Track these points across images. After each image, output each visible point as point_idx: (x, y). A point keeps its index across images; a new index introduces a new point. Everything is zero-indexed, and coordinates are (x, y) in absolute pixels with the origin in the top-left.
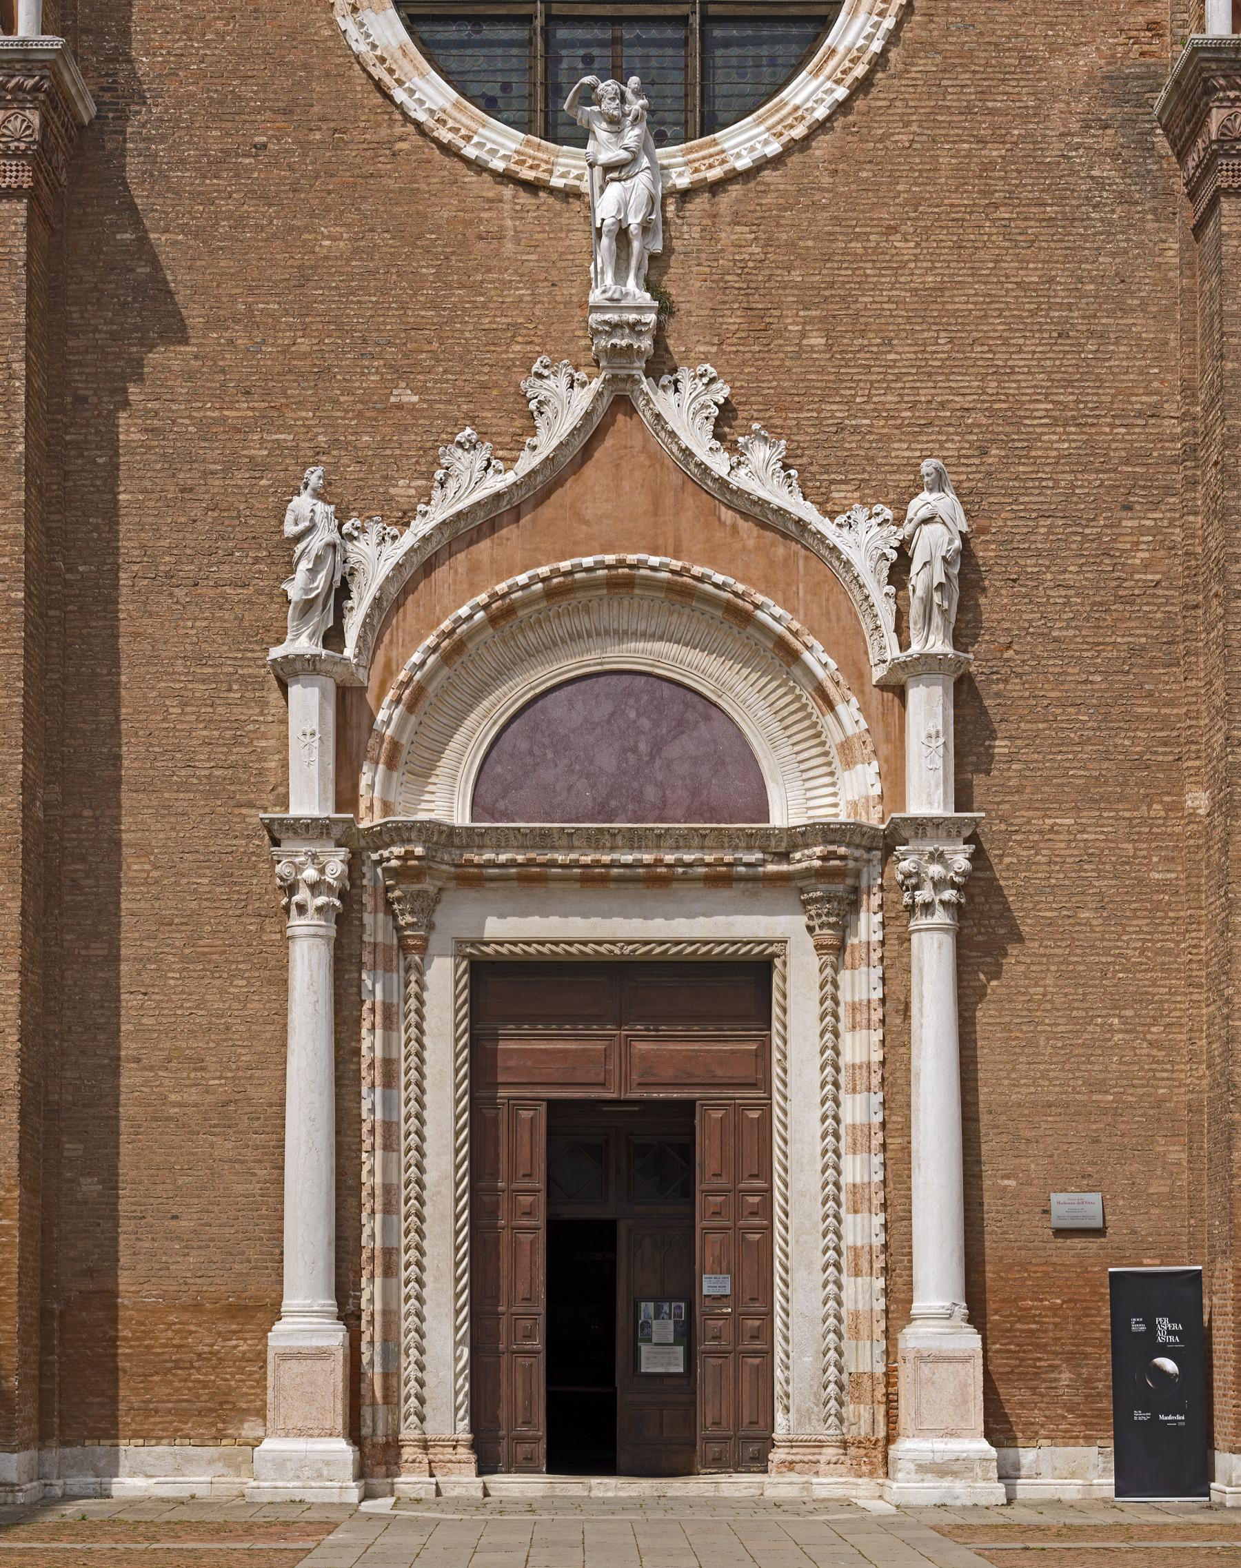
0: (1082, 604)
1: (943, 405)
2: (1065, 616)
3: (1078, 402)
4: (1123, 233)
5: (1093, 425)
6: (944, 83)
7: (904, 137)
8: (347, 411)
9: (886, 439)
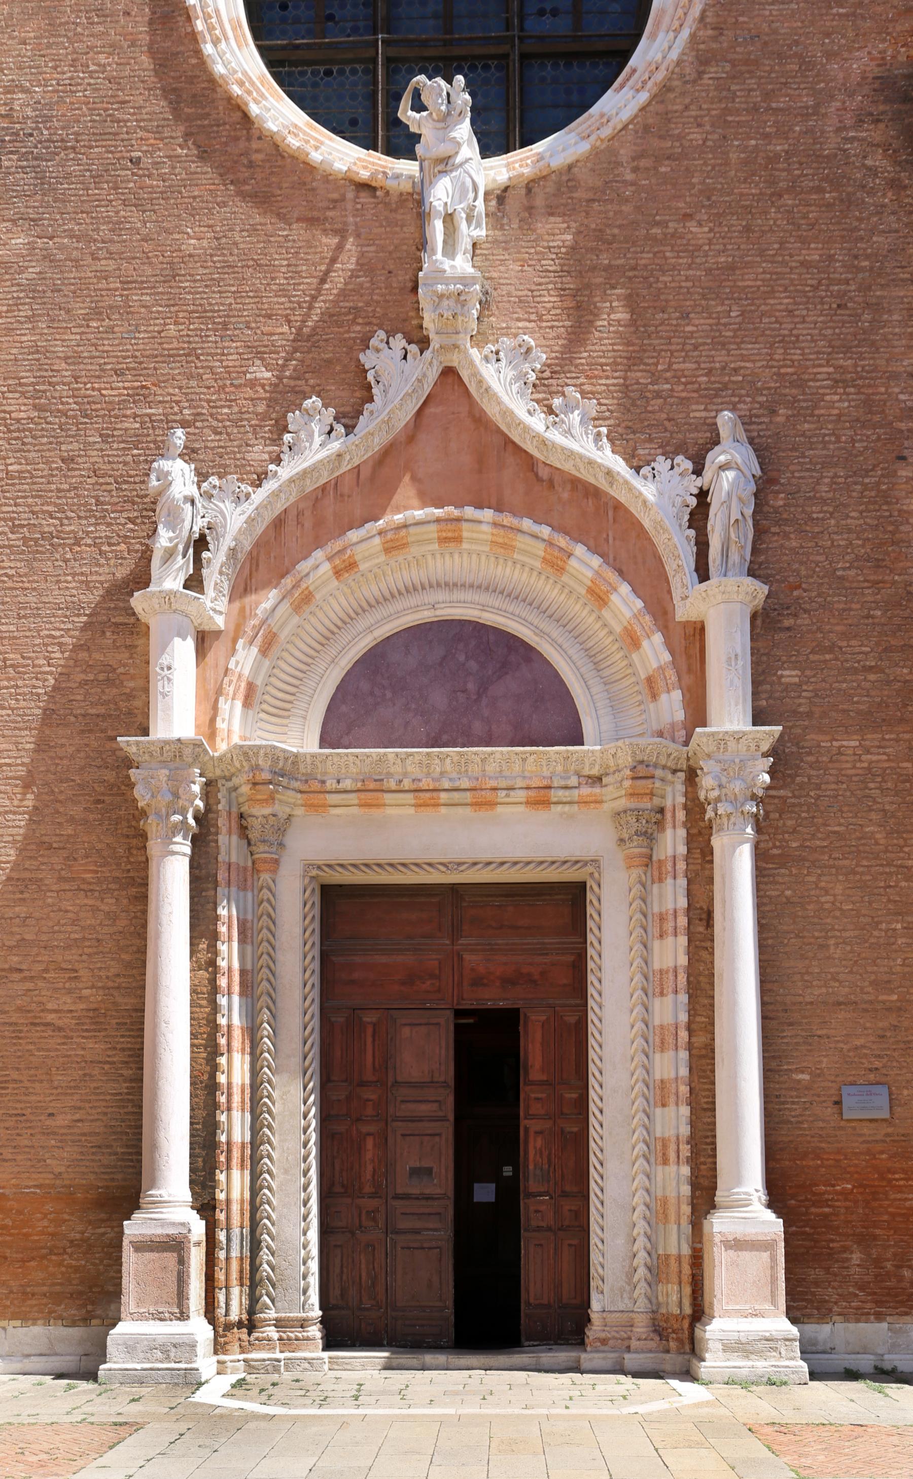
0: (863, 546)
1: (736, 370)
2: (847, 558)
3: (856, 365)
6: (733, 88)
7: (699, 137)
9: (684, 401)
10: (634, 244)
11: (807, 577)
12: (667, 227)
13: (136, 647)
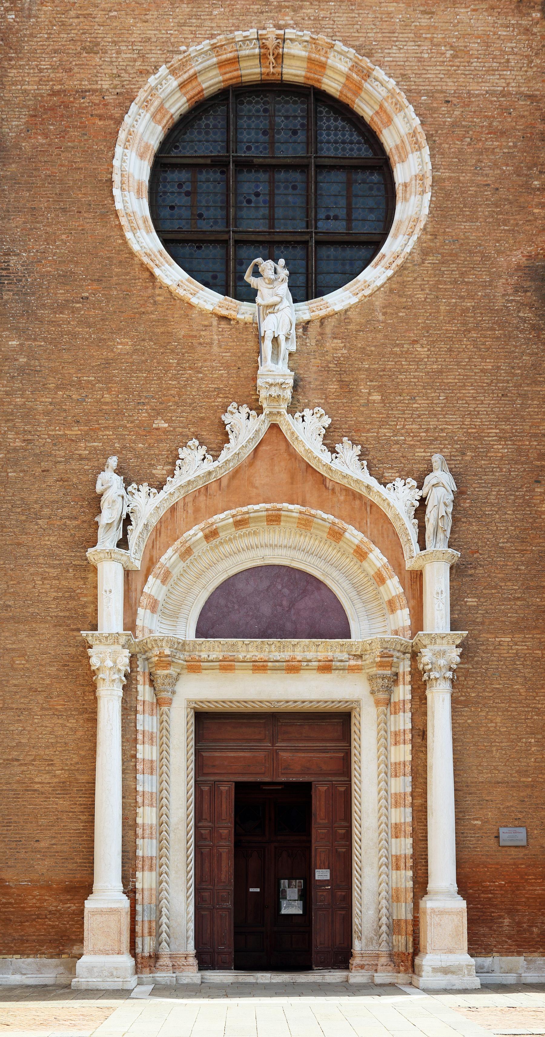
0: (515, 530)
2: (506, 536)
3: (512, 429)
4: (535, 344)
5: (520, 440)
6: (443, 269)
7: (422, 296)
8: (130, 432)
10: (383, 357)
11: (483, 547)
12: (403, 347)
13: (88, 578)
